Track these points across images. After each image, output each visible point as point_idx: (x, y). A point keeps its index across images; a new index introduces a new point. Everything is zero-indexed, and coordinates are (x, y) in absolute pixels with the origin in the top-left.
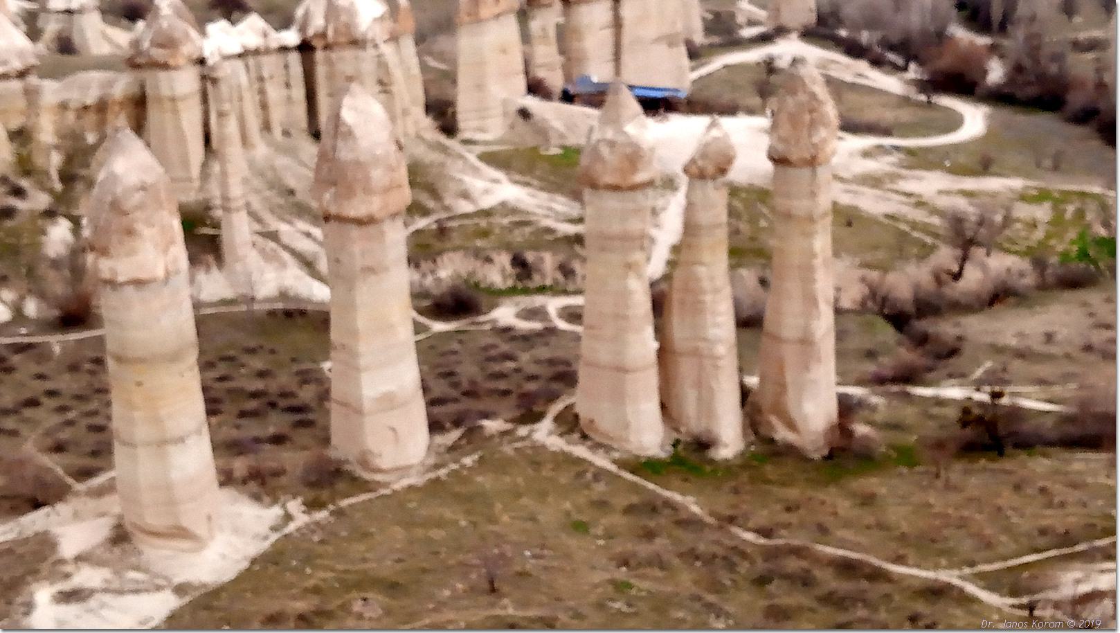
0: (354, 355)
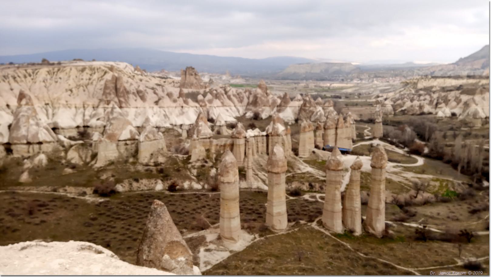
0: (272, 203)
